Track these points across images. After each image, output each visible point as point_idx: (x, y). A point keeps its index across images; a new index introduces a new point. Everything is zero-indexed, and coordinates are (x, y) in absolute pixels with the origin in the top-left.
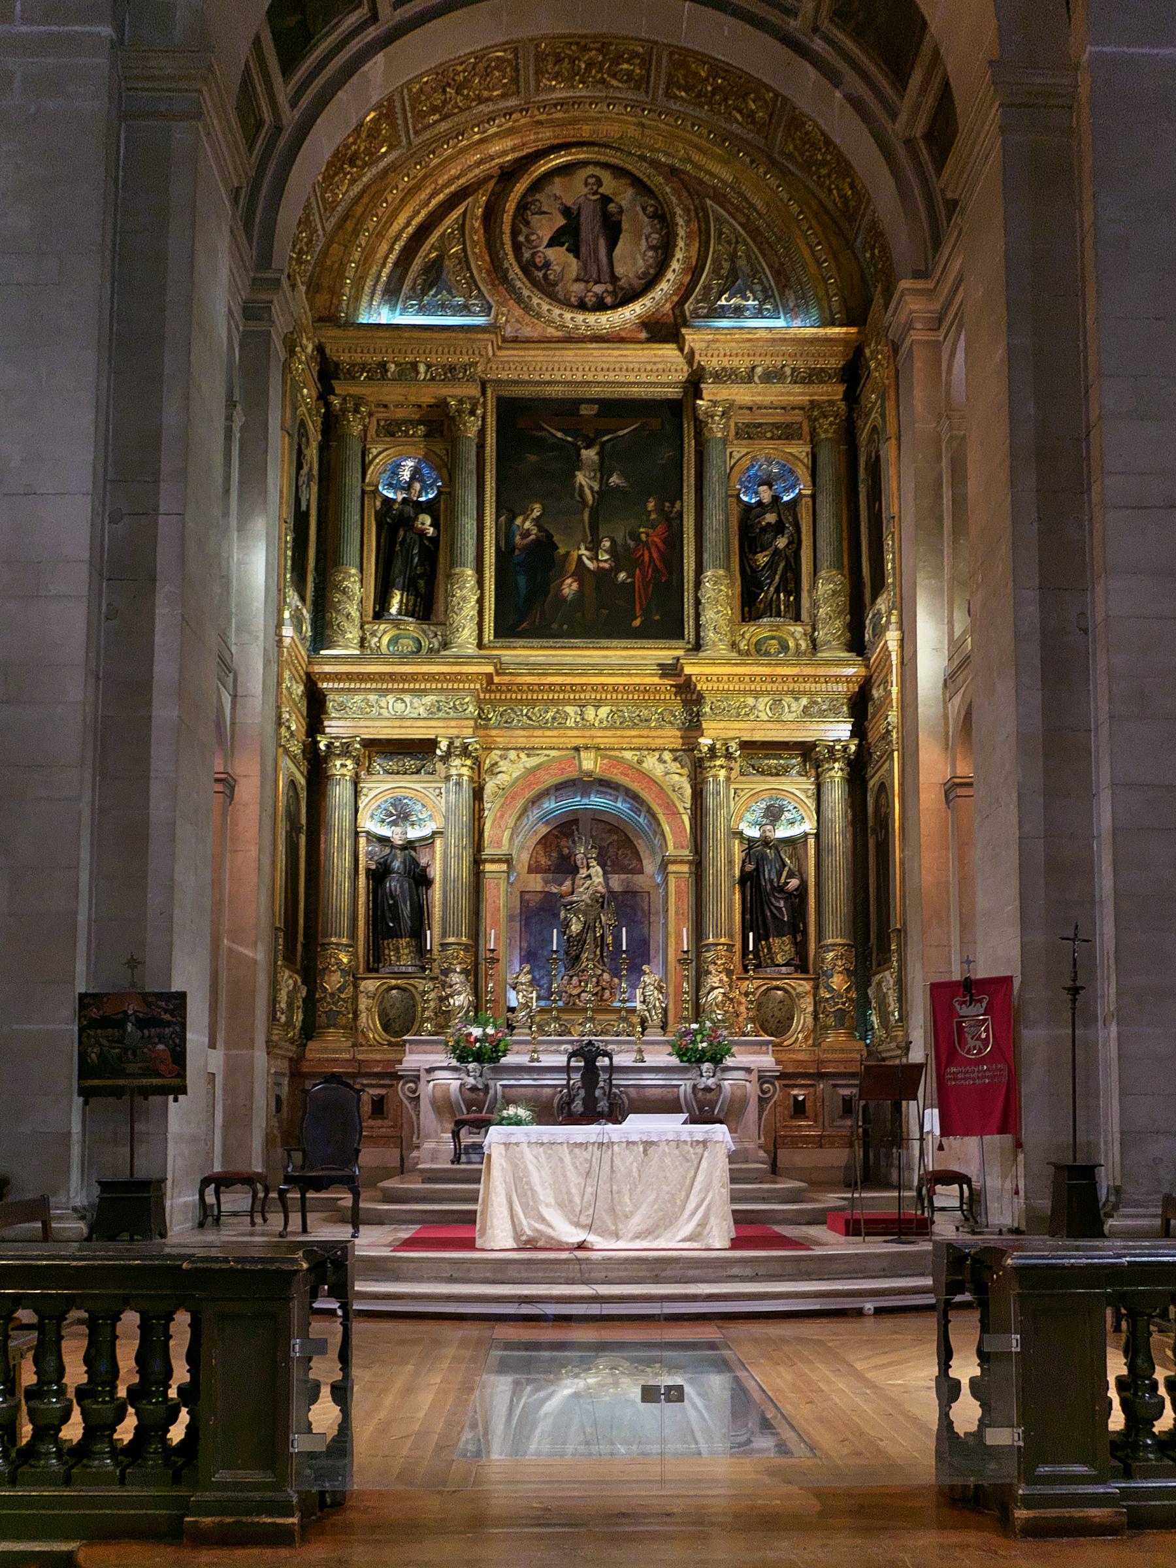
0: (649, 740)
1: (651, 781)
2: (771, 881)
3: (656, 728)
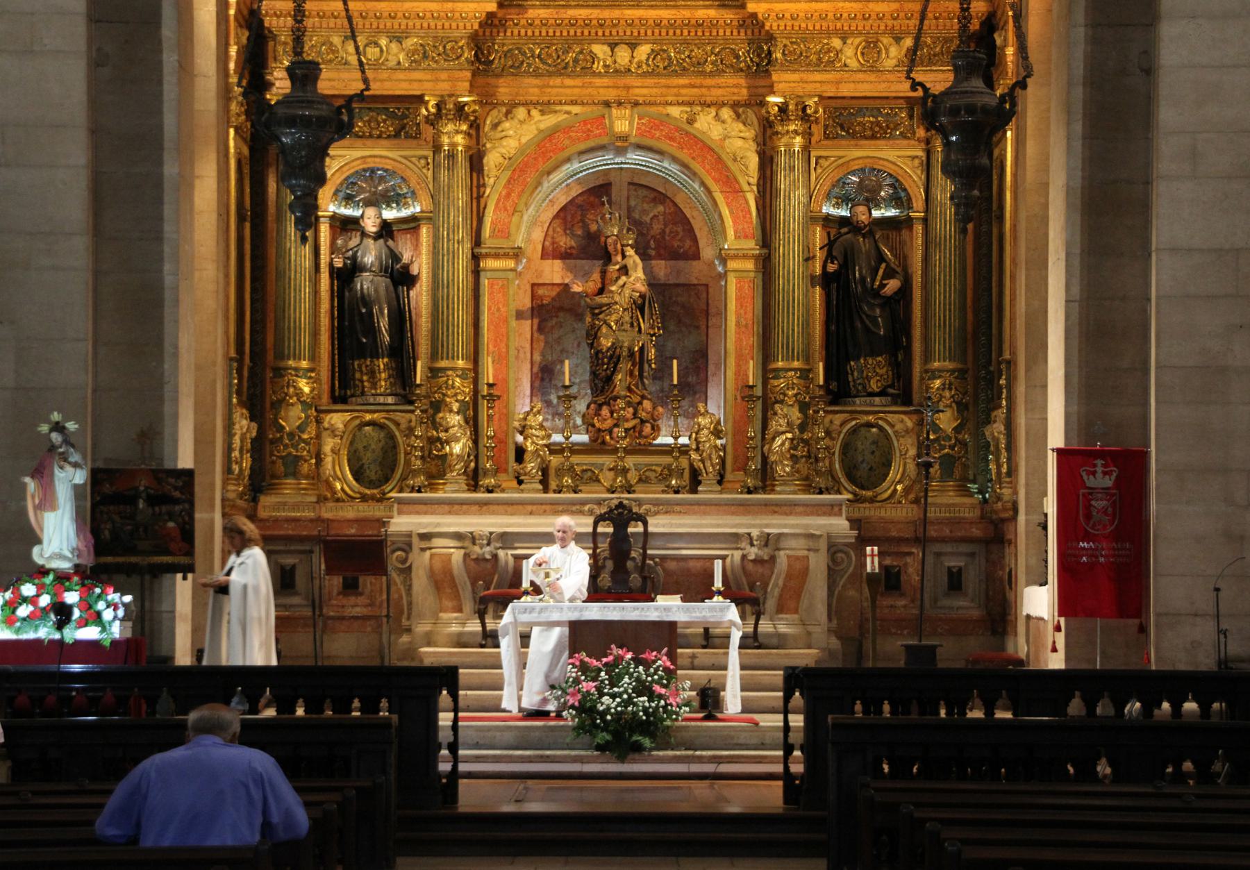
0: (704, 91)
1: (703, 147)
2: (863, 279)
3: (712, 75)
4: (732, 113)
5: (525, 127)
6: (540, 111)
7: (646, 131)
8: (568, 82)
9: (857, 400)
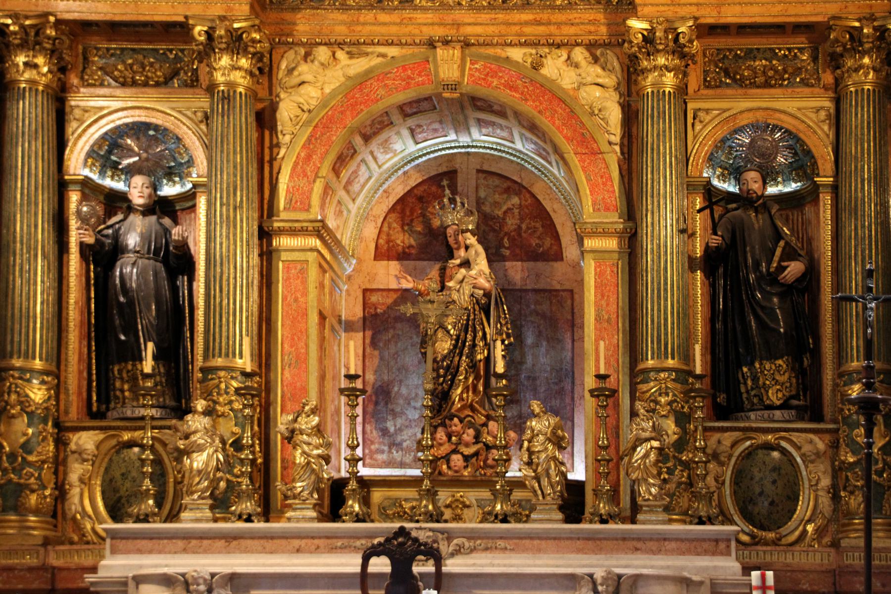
0: (553, 29)
2: (757, 264)
4: (587, 54)
5: (329, 73)
6: (348, 53)
7: (480, 79)
8: (383, 17)
9: (752, 415)
